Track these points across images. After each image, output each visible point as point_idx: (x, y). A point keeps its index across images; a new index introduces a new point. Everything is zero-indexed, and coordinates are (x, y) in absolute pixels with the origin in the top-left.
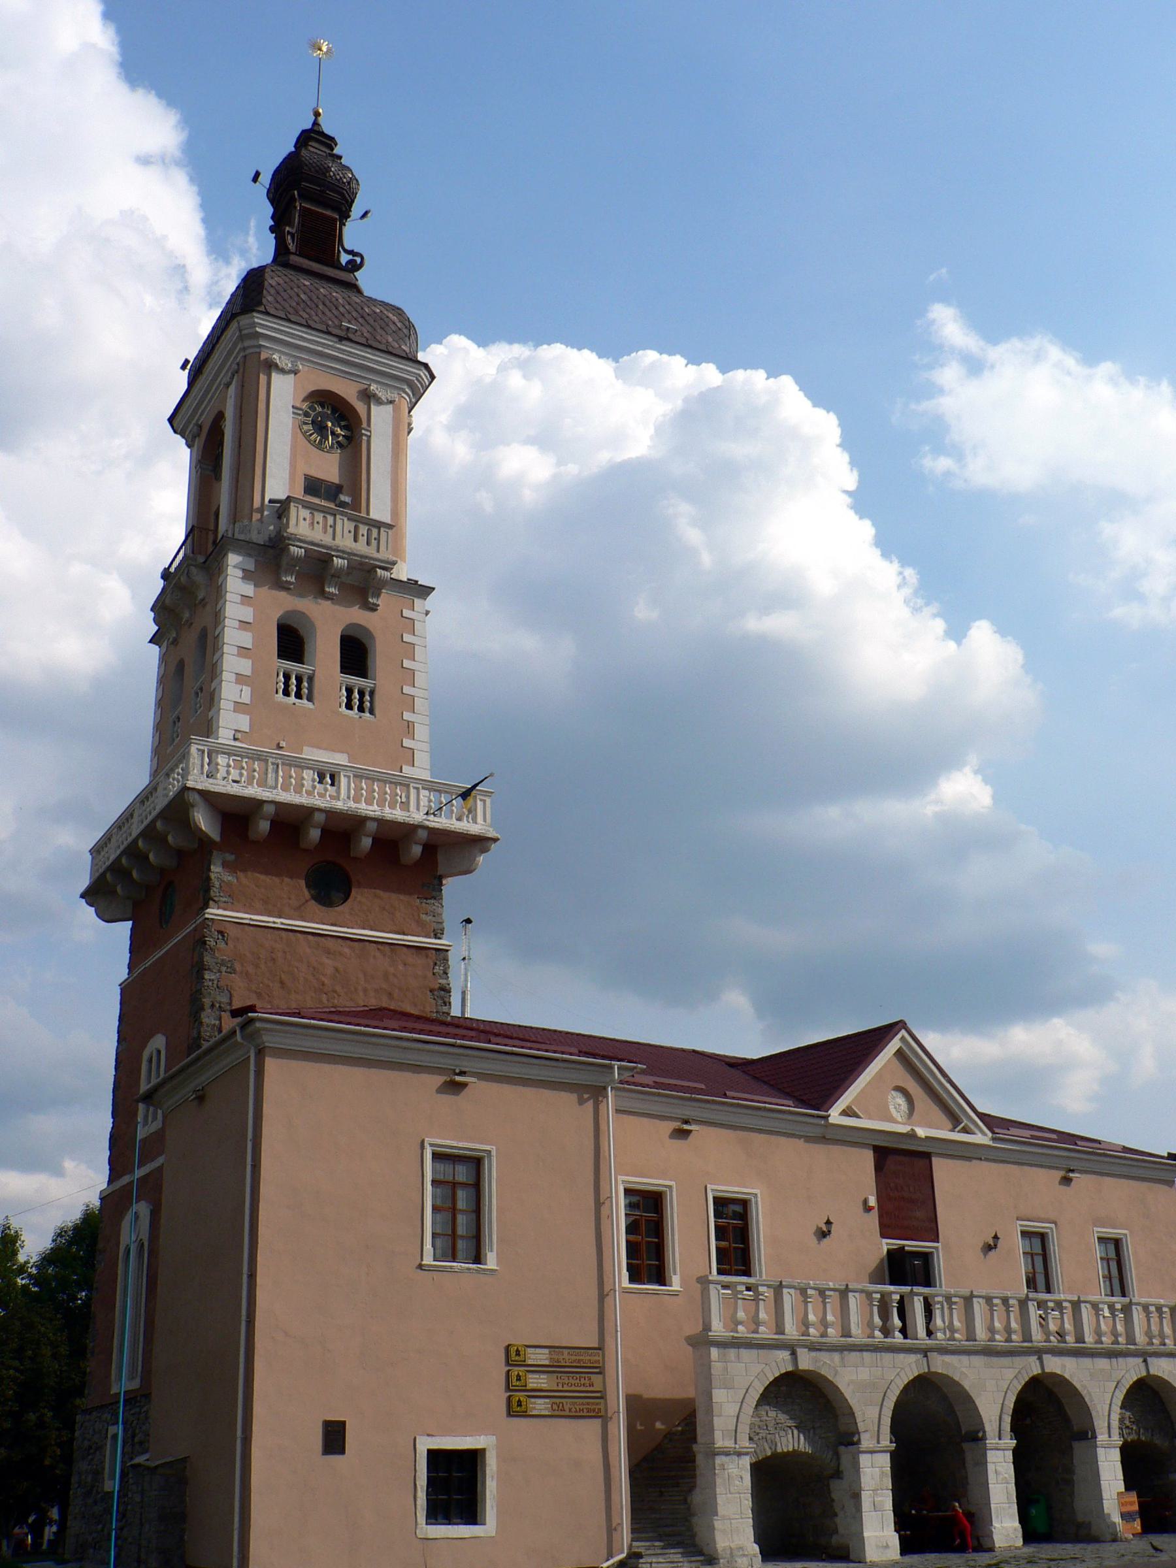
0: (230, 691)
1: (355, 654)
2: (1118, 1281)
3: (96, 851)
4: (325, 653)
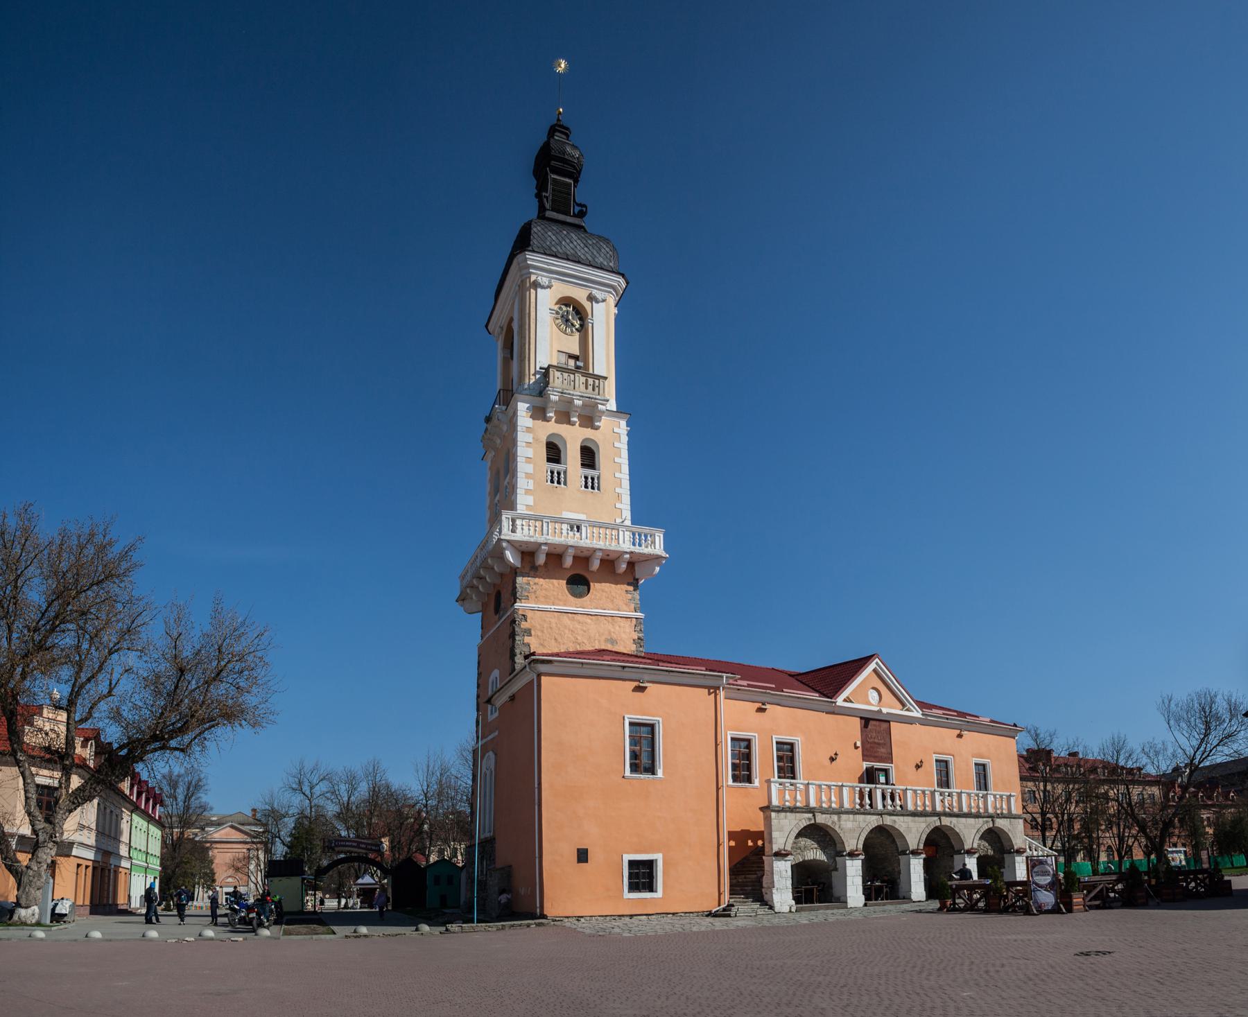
0: (523, 483)
1: (589, 456)
2: (983, 782)
4: (573, 456)
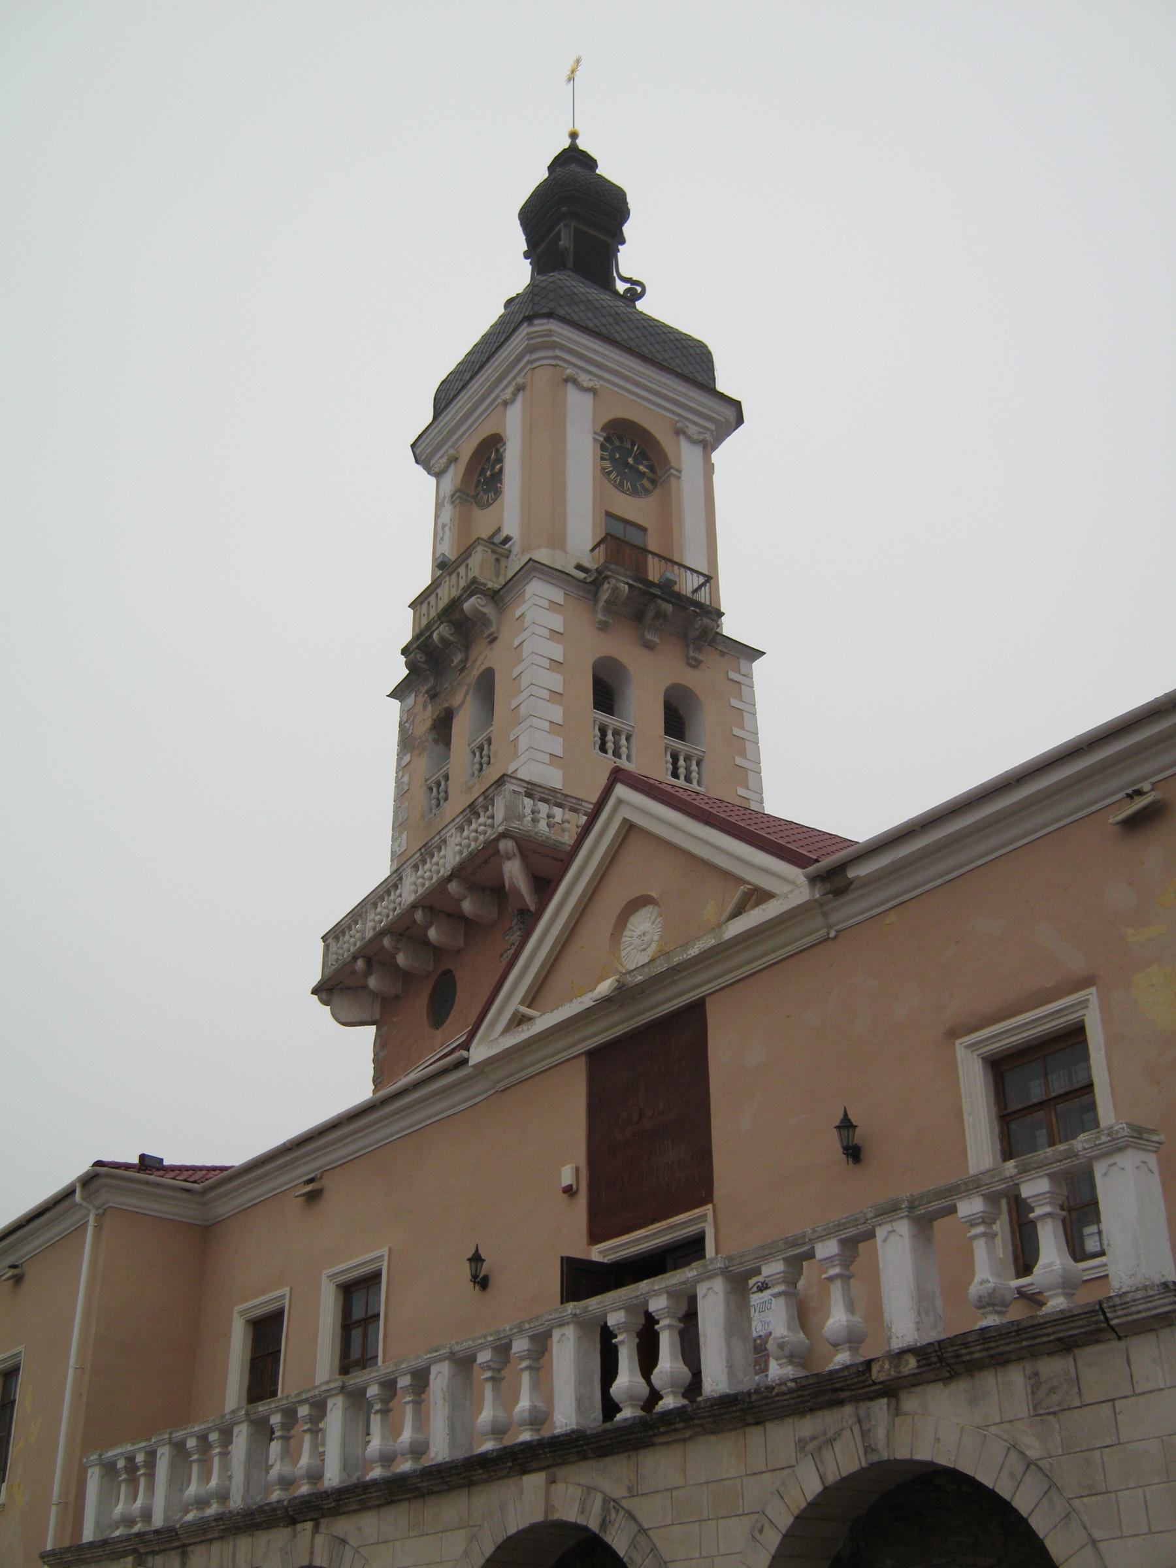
3: (333, 936)
